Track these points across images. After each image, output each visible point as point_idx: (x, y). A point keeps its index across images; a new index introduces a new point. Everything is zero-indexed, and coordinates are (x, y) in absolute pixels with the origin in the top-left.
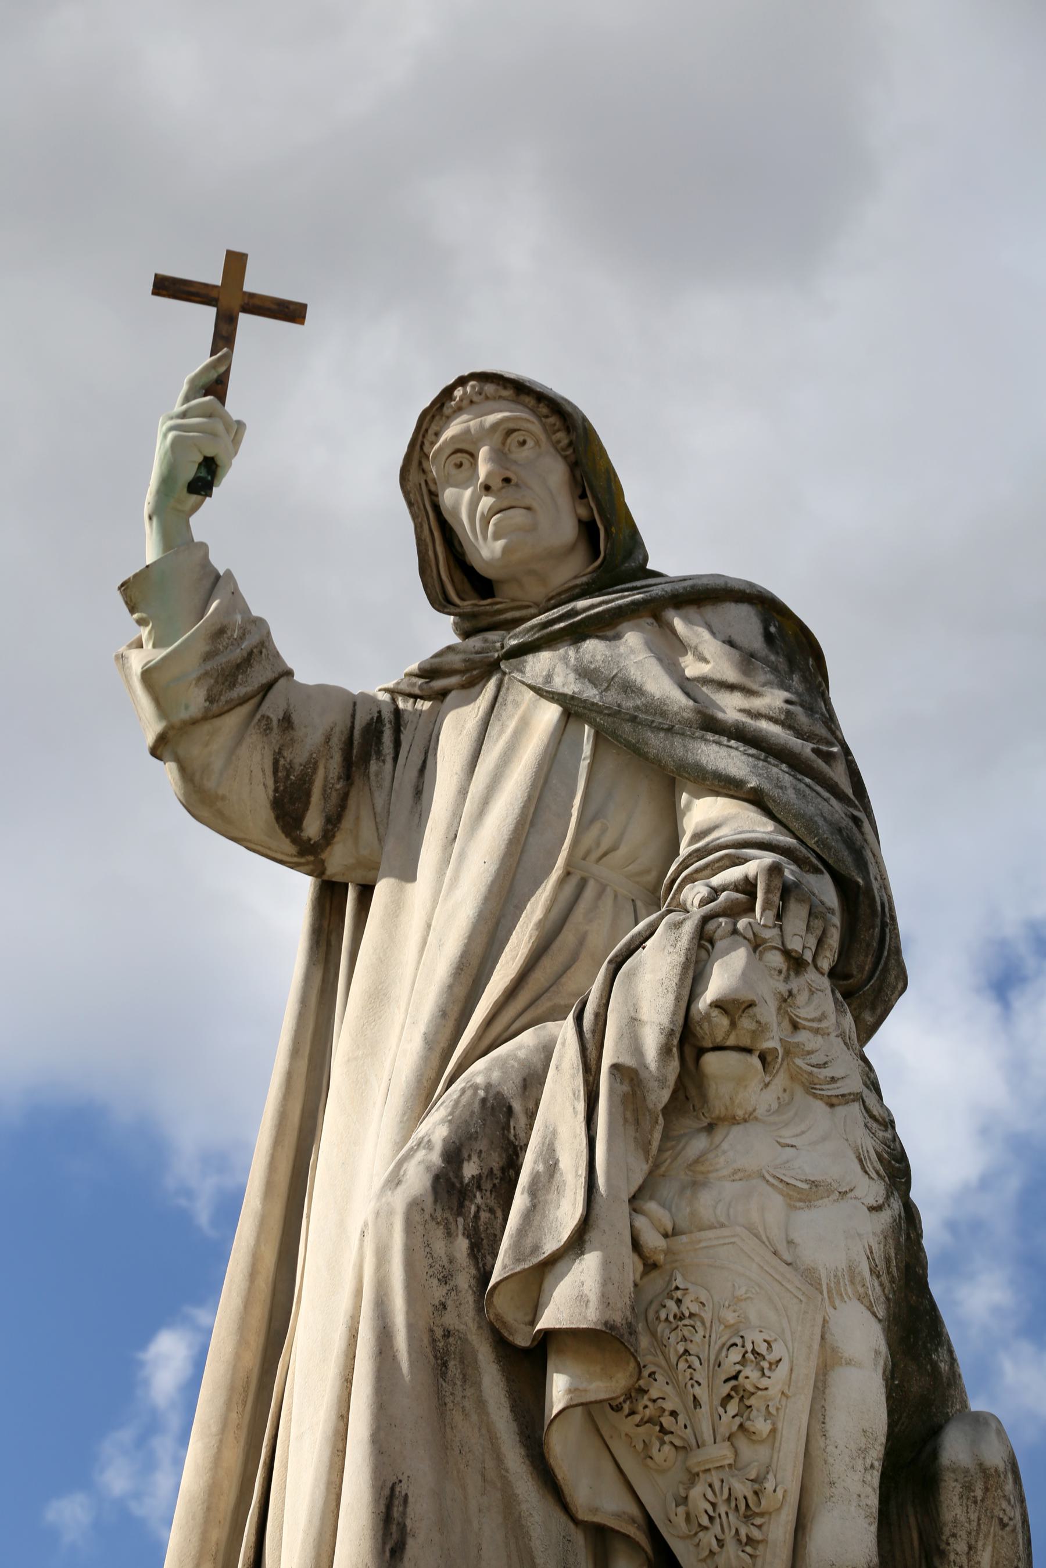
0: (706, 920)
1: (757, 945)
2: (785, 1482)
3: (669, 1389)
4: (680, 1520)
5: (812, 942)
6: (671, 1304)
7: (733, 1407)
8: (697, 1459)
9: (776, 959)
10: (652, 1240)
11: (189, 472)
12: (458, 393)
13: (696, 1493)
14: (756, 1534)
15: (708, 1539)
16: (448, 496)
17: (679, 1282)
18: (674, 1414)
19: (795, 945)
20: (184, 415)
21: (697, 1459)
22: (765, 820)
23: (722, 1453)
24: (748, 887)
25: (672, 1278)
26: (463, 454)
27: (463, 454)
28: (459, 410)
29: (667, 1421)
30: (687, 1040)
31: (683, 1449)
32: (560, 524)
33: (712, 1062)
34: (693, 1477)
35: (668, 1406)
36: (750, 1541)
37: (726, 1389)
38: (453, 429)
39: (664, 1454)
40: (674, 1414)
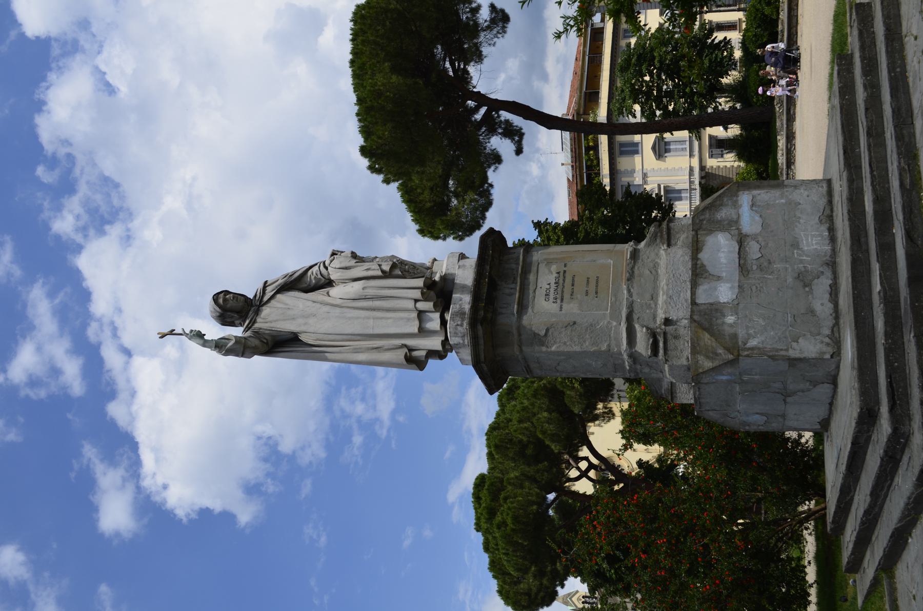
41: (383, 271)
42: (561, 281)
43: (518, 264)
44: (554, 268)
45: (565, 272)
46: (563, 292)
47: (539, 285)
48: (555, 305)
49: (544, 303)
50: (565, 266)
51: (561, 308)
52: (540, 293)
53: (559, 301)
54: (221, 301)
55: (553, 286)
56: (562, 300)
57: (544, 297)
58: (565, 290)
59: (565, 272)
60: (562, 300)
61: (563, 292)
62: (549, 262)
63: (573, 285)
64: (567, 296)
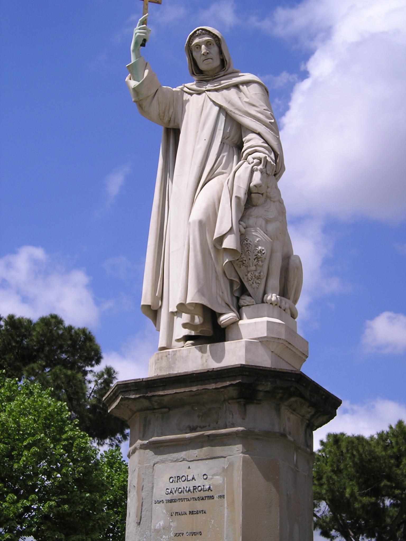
0: (253, 167)
1: (262, 172)
2: (264, 274)
3: (245, 256)
4: (246, 279)
5: (271, 171)
6: (245, 241)
7: (256, 260)
8: (249, 269)
9: (265, 175)
10: (243, 230)
11: (141, 42)
12: (197, 32)
13: (249, 275)
14: (259, 282)
15: (251, 282)
16: (195, 54)
17: (247, 237)
18: (245, 261)
19: (268, 172)
20: (140, 29)
21: (249, 269)
22: (261, 139)
23: (254, 268)
24: (260, 159)
25: (245, 237)
26: (198, 46)
27: (198, 46)
28: (197, 36)
29: (244, 262)
30: (249, 192)
31: (247, 267)
32: (217, 63)
33: (253, 195)
34: (248, 272)
35: (244, 259)
36: (258, 283)
37: (255, 257)
38: (197, 41)
39: (243, 268)
40: (245, 261)
41: (221, 239)
42: (197, 495)
43: (226, 427)
44: (218, 480)
45: (212, 497)
46: (181, 500)
47: (192, 465)
48: (164, 493)
49: (166, 478)
50: (222, 497)
51: (159, 502)
52: (181, 469)
53: (169, 497)
54: (197, 41)
55: (190, 485)
56: (171, 501)
57: (174, 474)
58: (186, 502)
59: (212, 497)
60: (171, 501)
61: (181, 500)
62: (227, 472)
63: (191, 513)
64: (177, 507)
